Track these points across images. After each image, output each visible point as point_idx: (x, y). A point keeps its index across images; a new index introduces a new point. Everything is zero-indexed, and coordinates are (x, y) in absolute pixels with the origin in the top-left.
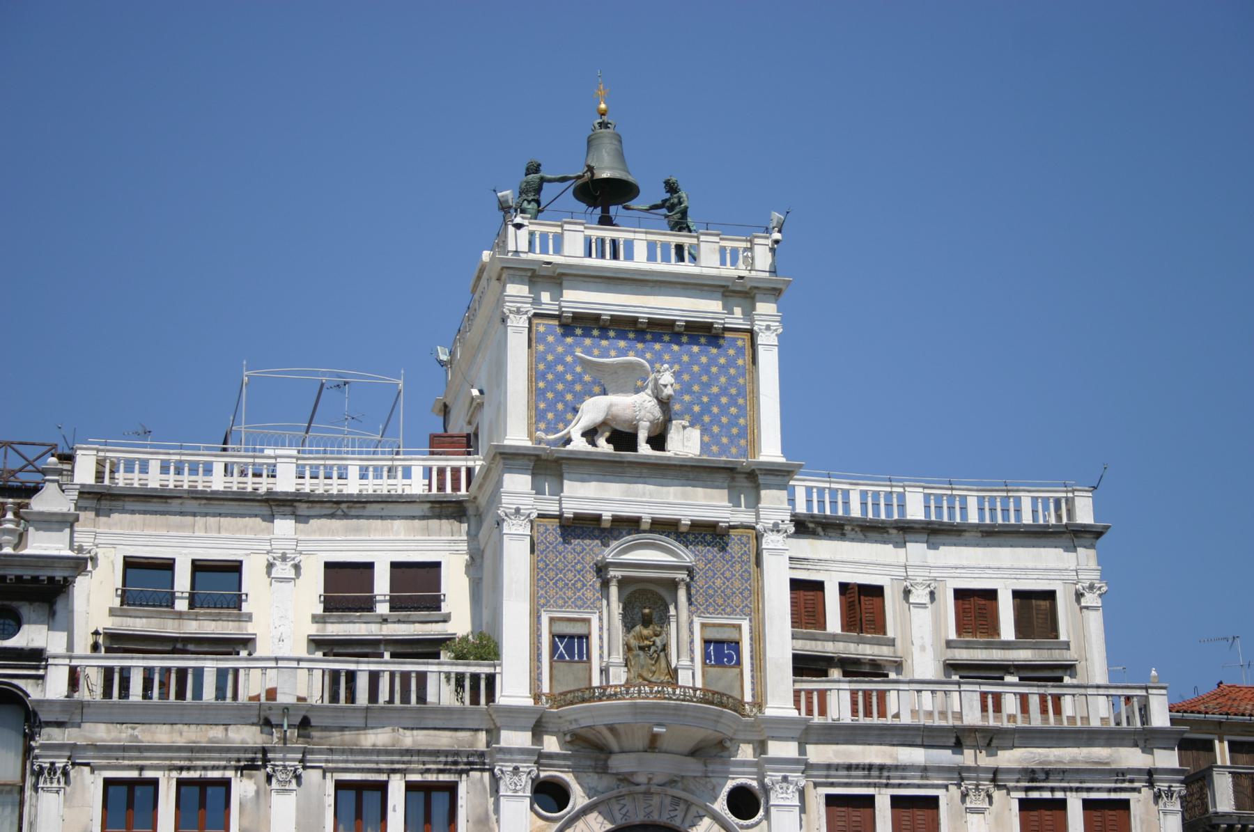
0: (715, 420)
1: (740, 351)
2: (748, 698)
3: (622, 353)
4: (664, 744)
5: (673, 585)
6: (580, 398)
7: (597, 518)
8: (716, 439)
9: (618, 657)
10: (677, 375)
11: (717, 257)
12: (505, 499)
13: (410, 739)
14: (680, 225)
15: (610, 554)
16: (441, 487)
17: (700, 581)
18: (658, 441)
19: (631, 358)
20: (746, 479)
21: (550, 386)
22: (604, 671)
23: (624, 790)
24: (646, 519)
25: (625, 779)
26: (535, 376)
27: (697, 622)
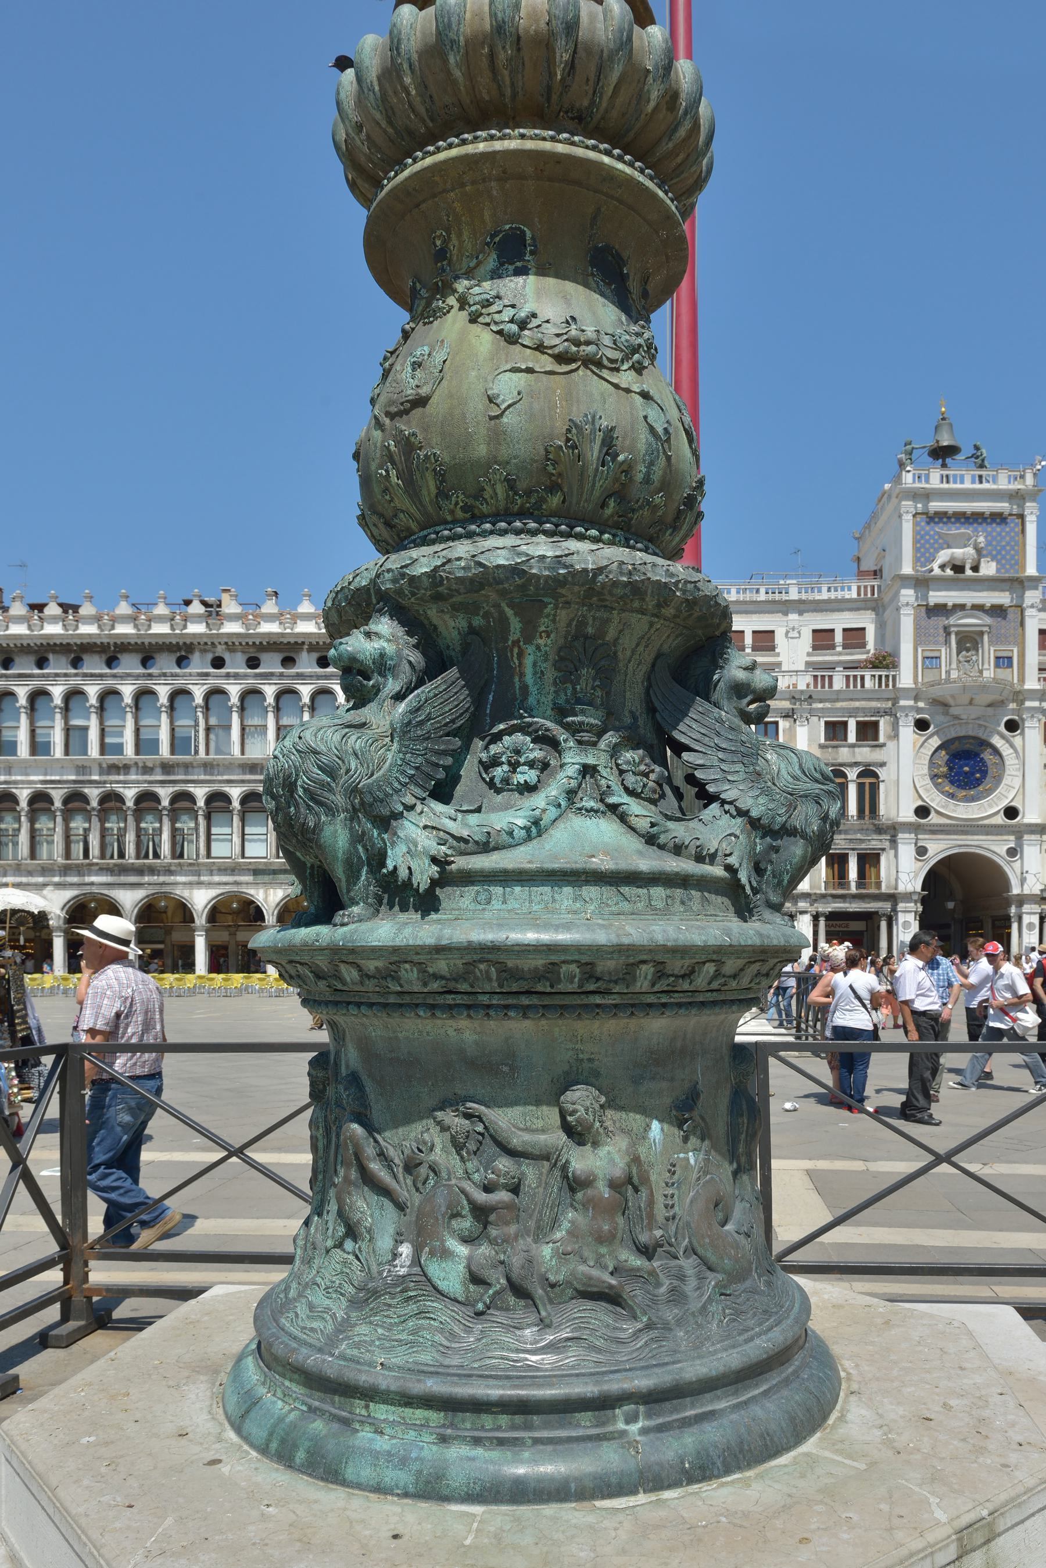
0: (1004, 557)
1: (1017, 525)
2: (1016, 681)
3: (958, 529)
4: (975, 702)
5: (982, 633)
6: (937, 551)
7: (945, 605)
8: (1003, 566)
9: (954, 666)
10: (986, 537)
11: (1006, 480)
12: (901, 599)
13: (857, 704)
14: (982, 466)
15: (952, 621)
16: (866, 594)
17: (994, 631)
18: (975, 569)
19: (963, 531)
20: (1018, 584)
21: (923, 546)
22: (948, 672)
23: (956, 722)
24: (969, 605)
25: (957, 717)
26: (916, 541)
27: (992, 649)
